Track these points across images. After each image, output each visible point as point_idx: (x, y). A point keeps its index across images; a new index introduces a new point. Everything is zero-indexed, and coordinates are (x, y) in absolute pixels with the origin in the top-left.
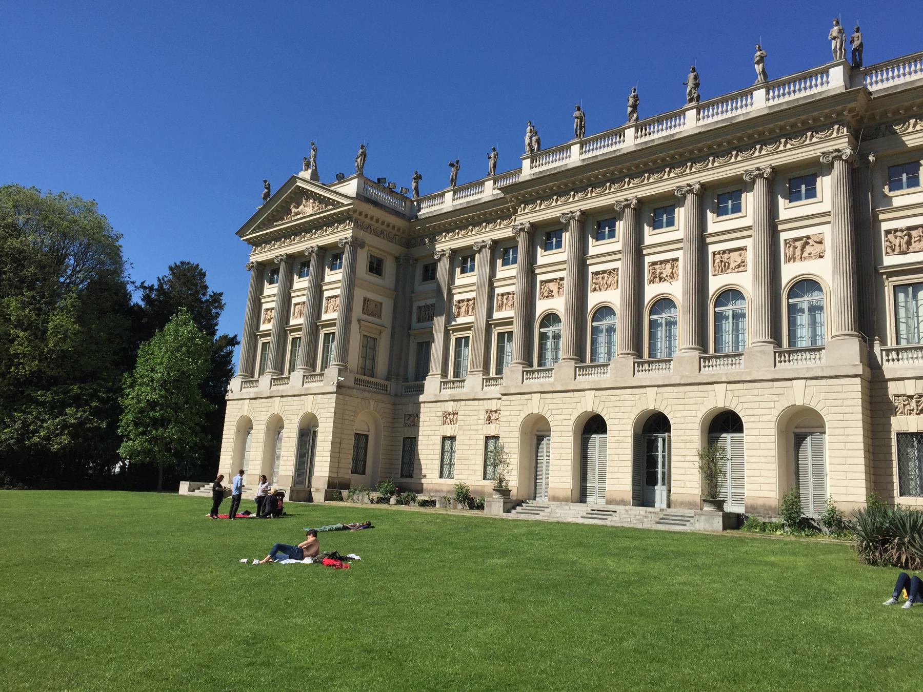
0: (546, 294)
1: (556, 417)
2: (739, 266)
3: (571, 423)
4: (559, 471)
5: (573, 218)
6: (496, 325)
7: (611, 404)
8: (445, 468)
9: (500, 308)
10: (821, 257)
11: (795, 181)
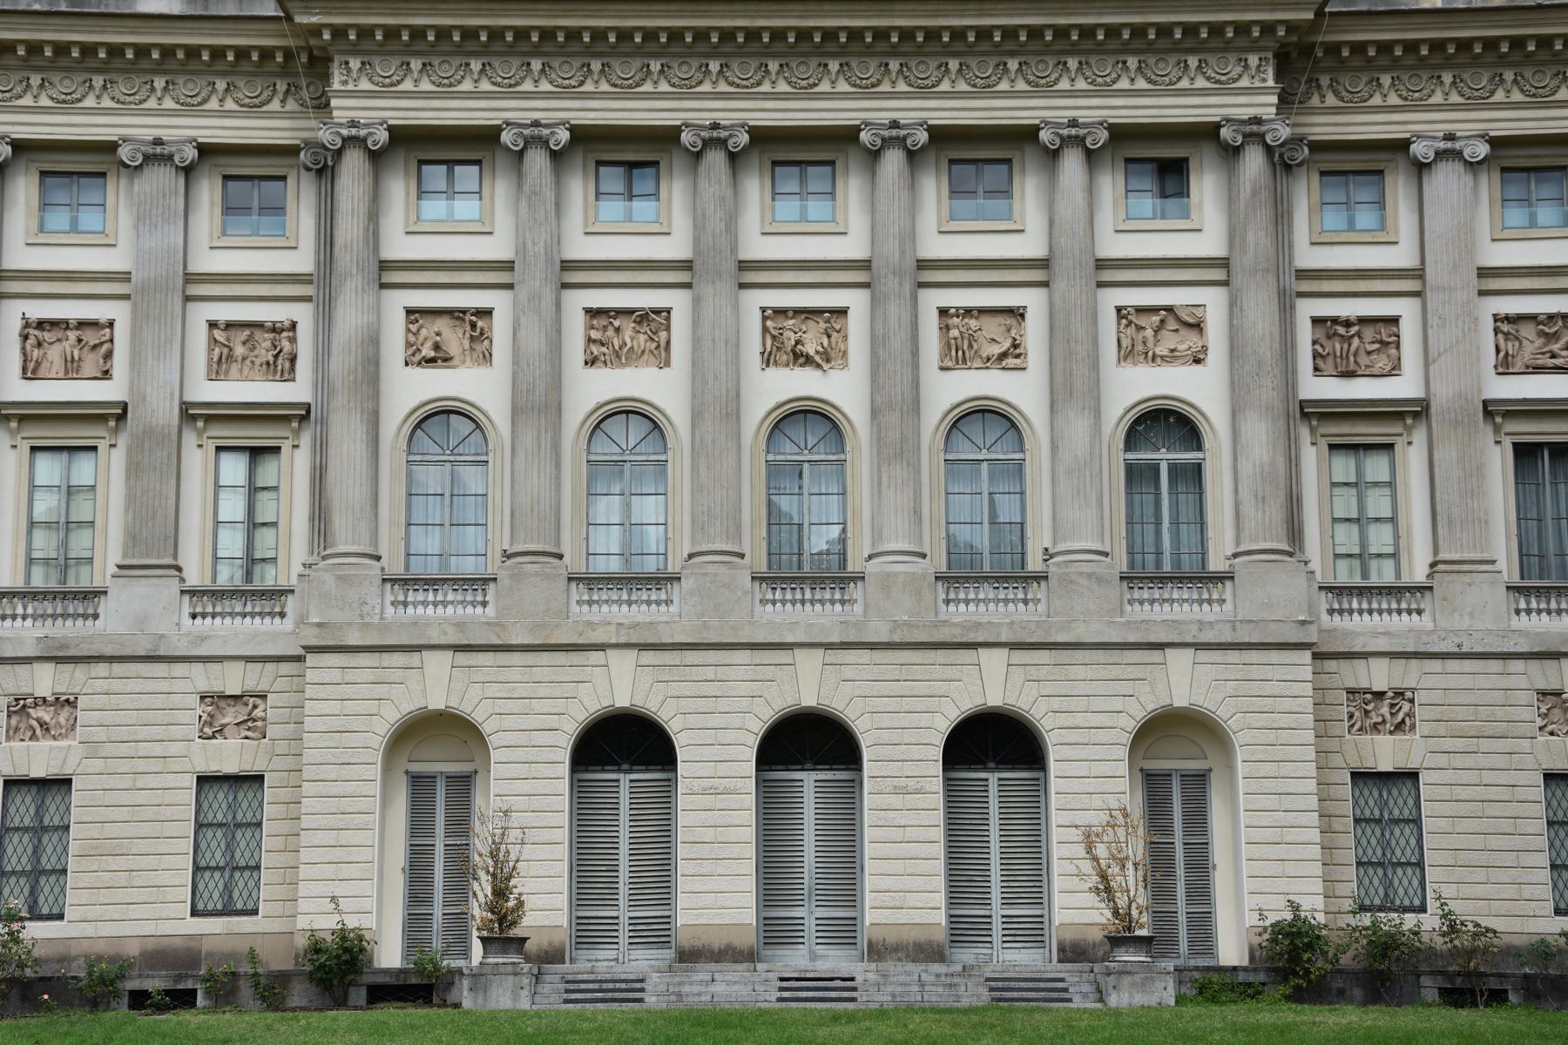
0: (428, 352)
1: (510, 722)
2: (1004, 355)
7: (687, 689)
10: (1197, 361)
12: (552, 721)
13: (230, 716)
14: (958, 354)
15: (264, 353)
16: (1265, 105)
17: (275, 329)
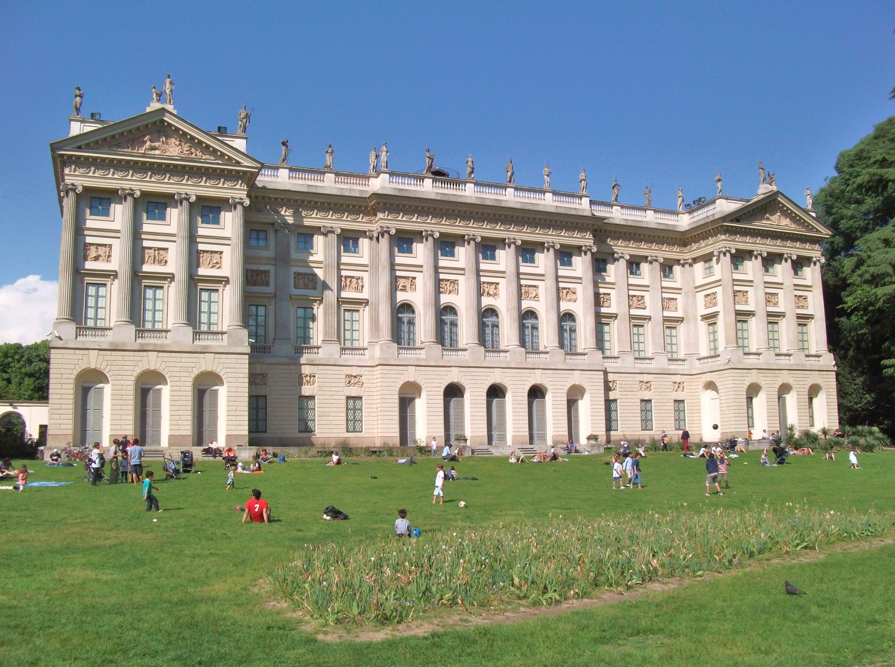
3: (191, 379)
4: (473, 425)
6: (344, 303)
11: (565, 255)
12: (439, 385)
16: (590, 242)
17: (358, 279)
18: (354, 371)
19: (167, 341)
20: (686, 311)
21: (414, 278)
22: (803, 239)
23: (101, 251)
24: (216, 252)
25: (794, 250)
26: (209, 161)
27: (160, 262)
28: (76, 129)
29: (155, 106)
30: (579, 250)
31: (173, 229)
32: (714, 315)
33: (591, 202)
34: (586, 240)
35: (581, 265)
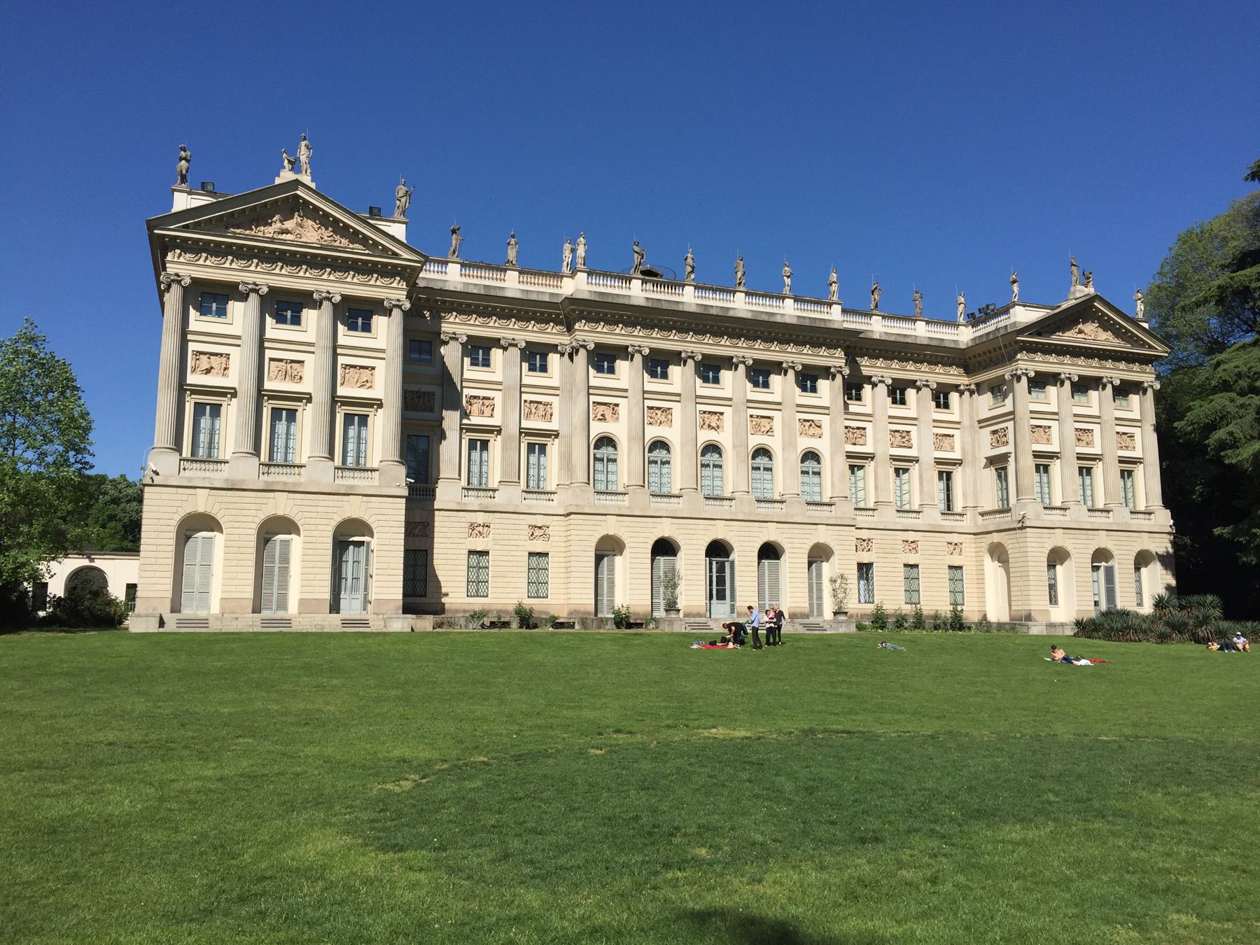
5: (640, 352)
8: (477, 584)
9: (527, 417)
13: (538, 532)
14: (757, 430)
15: (541, 412)
17: (546, 404)
18: (539, 521)
19: (302, 479)
20: (963, 450)
21: (617, 405)
22: (1130, 358)
23: (215, 361)
24: (366, 368)
25: (1116, 373)
26: (358, 252)
27: (293, 378)
28: (182, 202)
29: (286, 176)
30: (826, 372)
31: (310, 337)
32: (1005, 457)
33: (844, 311)
34: (835, 359)
35: (828, 391)
